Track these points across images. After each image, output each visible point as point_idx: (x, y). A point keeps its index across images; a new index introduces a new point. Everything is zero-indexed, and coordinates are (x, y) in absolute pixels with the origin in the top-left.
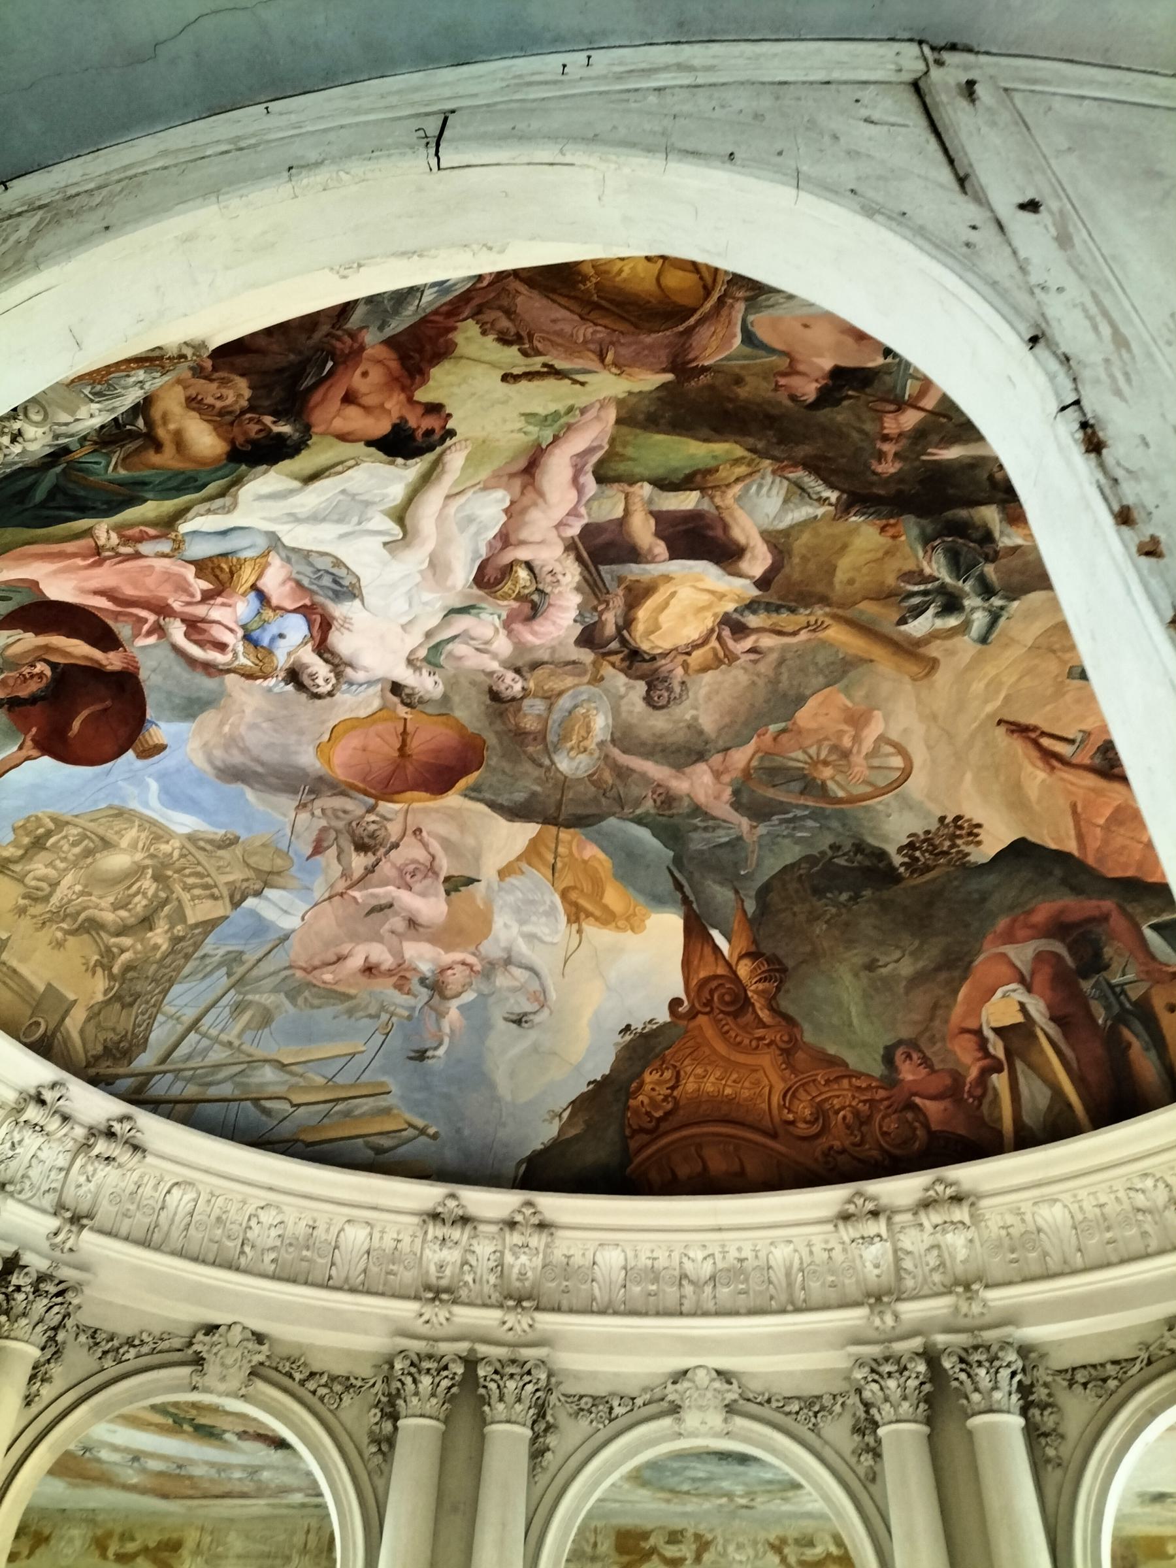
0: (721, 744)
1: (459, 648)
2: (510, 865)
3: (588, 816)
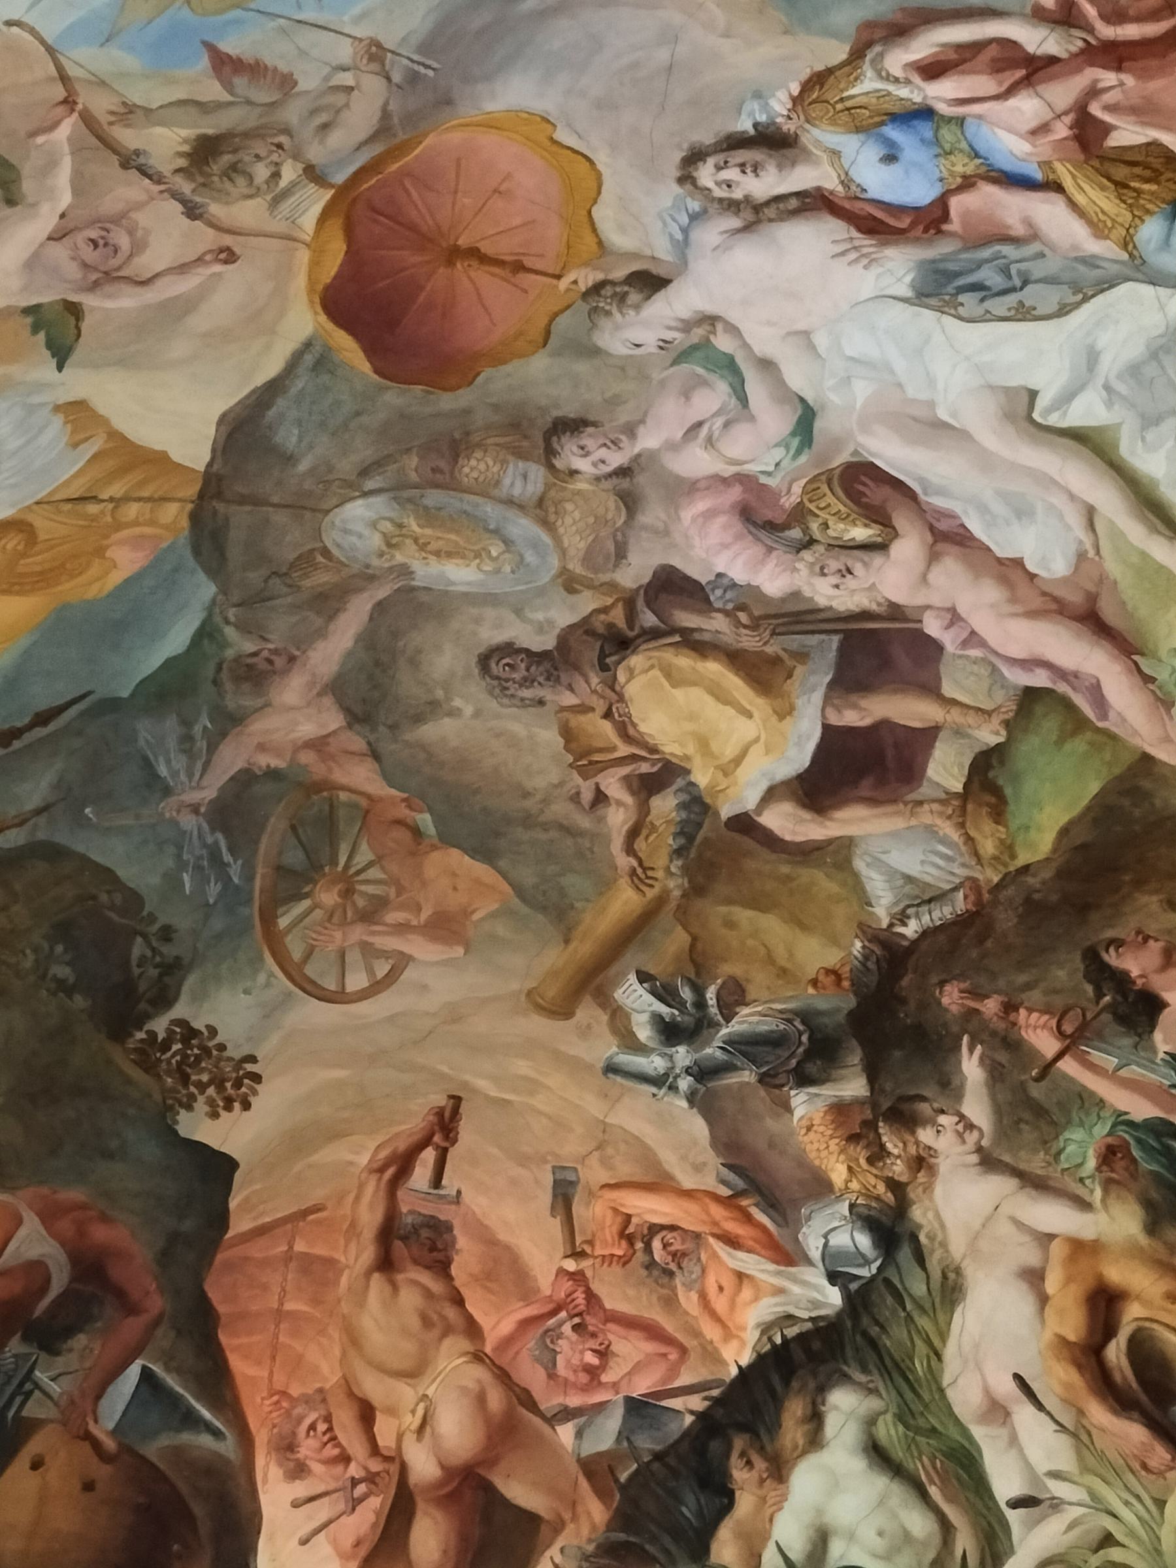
0: (387, 747)
3: (220, 550)
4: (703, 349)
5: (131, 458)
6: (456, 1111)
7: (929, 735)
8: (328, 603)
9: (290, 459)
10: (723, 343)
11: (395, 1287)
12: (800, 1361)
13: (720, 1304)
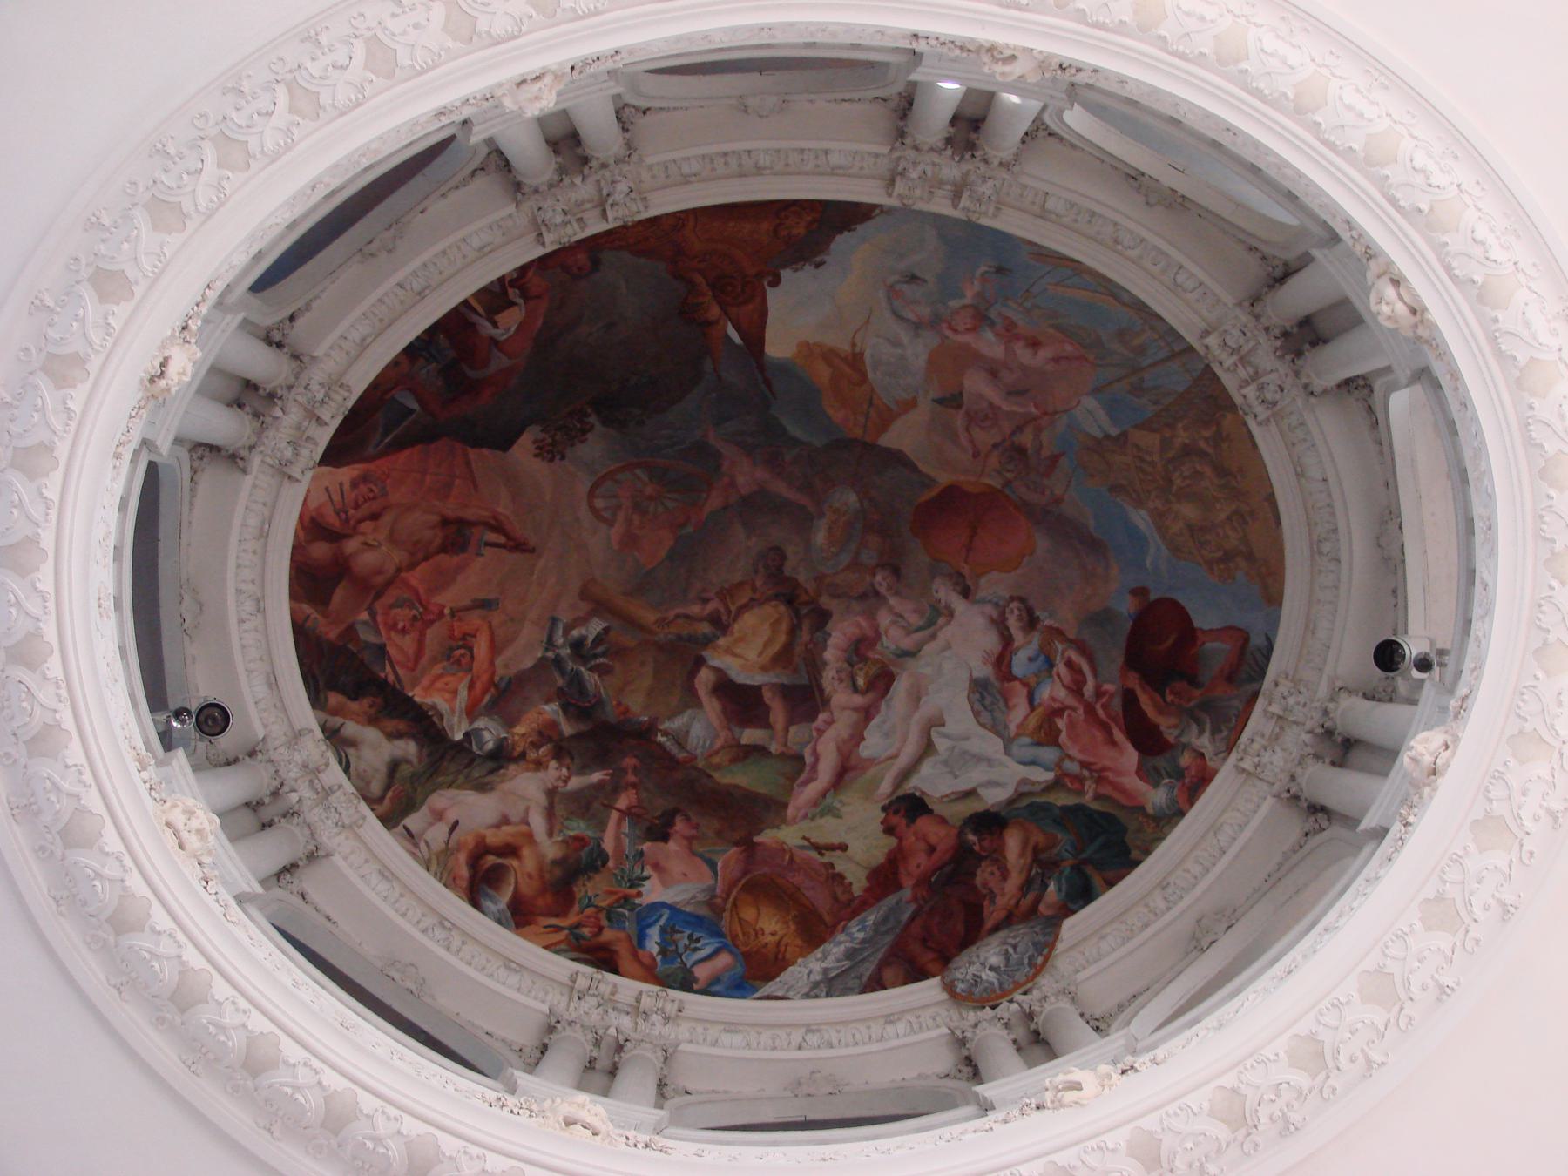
1: (915, 620)
2: (906, 411)
4: (937, 615)
5: (886, 419)
6: (525, 551)
7: (767, 725)
10: (941, 621)
11: (433, 527)
12: (424, 726)
13: (439, 685)
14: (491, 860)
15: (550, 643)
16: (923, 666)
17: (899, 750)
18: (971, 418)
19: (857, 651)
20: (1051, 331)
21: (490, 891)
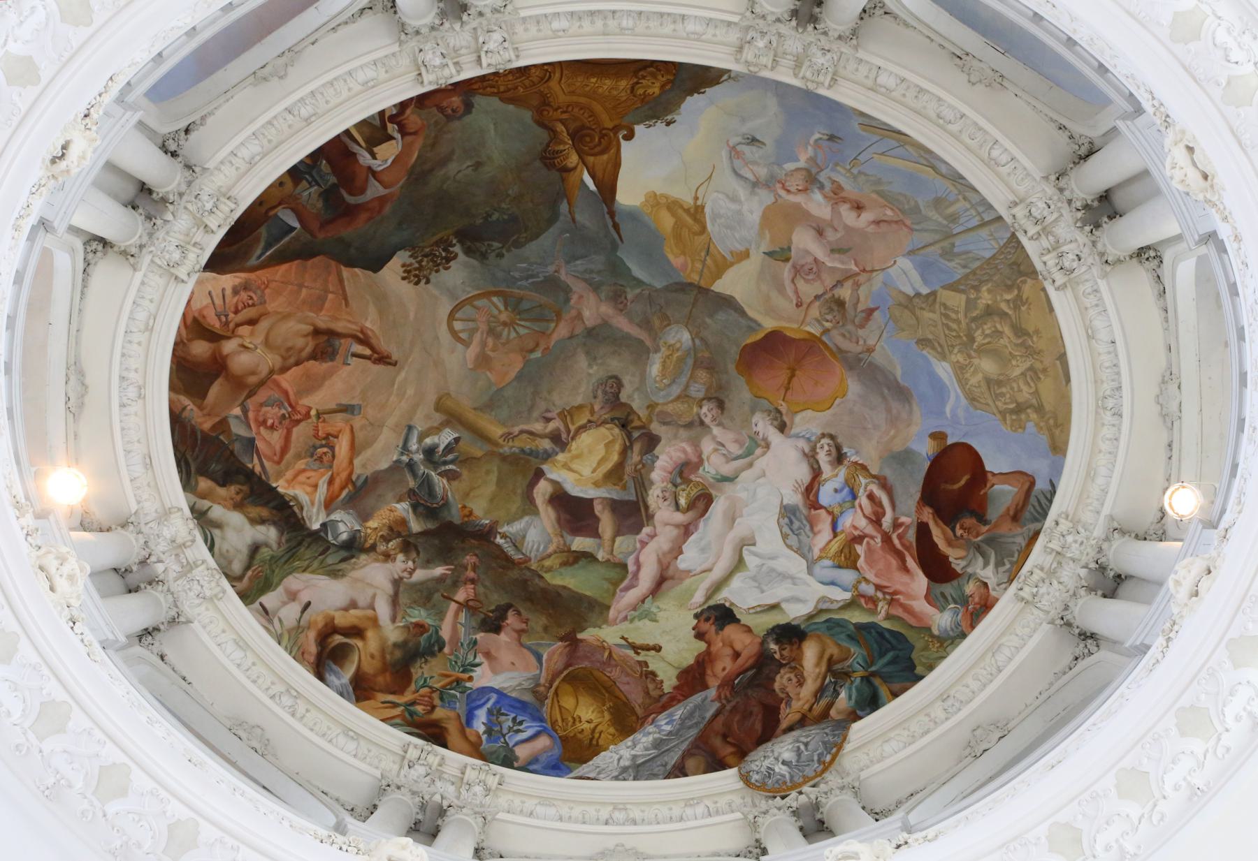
1: (735, 449)
3: (676, 291)
4: (755, 445)
5: (722, 267)
6: (390, 364)
7: (595, 534)
8: (646, 324)
9: (711, 316)
10: (758, 451)
12: (284, 514)
13: (302, 478)
14: (338, 639)
15: (405, 448)
16: (738, 490)
17: (714, 564)
18: (797, 271)
19: (681, 474)
20: (874, 196)
21: (334, 667)
